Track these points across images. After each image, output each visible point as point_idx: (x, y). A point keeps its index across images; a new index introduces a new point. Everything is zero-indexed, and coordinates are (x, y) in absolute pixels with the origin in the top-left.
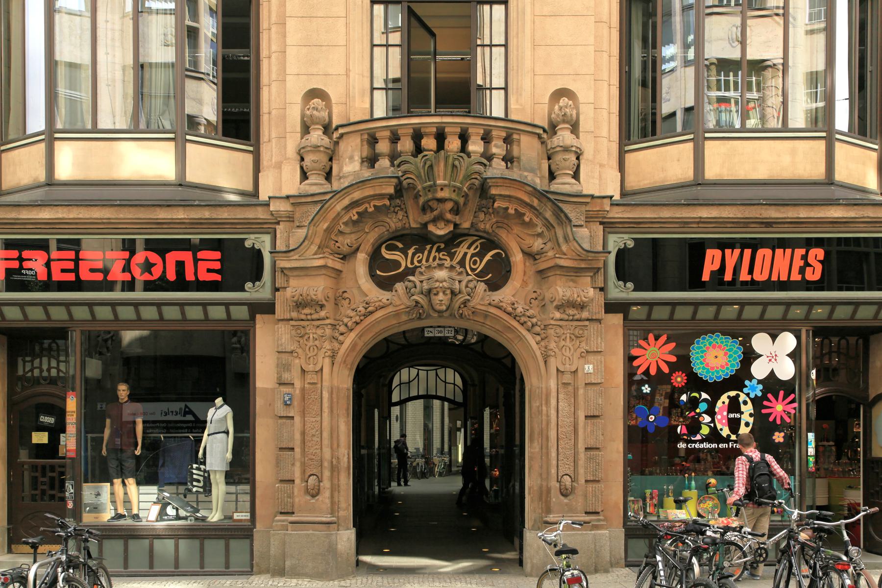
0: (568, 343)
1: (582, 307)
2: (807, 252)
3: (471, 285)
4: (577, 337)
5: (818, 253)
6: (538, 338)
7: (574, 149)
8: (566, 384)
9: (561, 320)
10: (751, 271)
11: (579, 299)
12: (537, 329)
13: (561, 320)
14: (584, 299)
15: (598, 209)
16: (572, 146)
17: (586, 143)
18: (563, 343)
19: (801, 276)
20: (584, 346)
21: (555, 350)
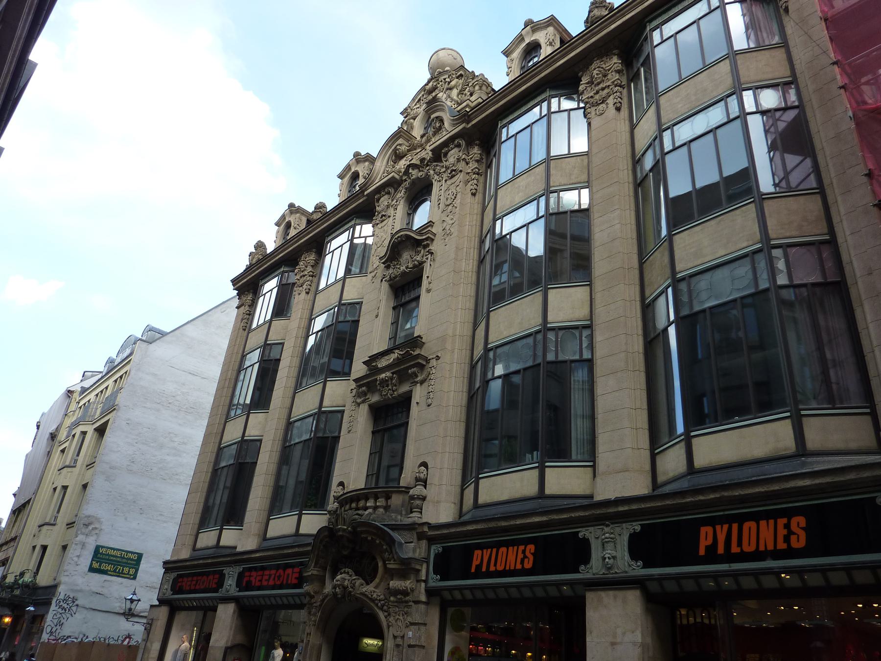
0: (401, 618)
1: (405, 593)
2: (525, 548)
3: (353, 582)
4: (406, 614)
5: (531, 548)
6: (386, 614)
7: (416, 496)
8: (398, 646)
9: (396, 602)
10: (495, 565)
11: (401, 589)
12: (385, 608)
13: (396, 602)
14: (404, 588)
15: (421, 531)
16: (414, 495)
17: (430, 492)
18: (397, 617)
19: (521, 565)
20: (409, 619)
21: (392, 621)
